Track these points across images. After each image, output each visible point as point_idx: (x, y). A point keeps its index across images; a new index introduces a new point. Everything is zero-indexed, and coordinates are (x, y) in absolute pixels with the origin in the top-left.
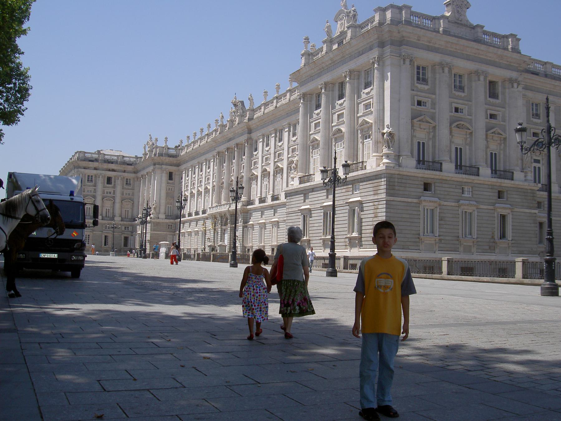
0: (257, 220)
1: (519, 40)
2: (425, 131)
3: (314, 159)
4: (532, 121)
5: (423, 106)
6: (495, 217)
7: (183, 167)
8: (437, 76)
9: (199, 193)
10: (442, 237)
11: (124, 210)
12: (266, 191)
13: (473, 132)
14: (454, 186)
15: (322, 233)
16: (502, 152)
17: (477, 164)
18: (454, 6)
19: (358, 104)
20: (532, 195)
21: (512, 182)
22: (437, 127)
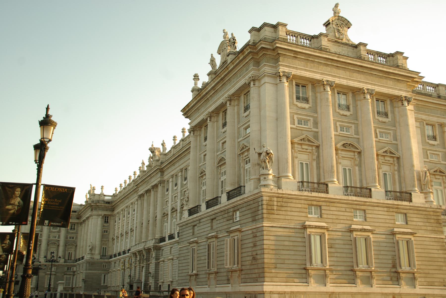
0: (167, 256)
1: (406, 58)
2: (308, 151)
3: (204, 190)
4: (428, 143)
5: (305, 125)
6: (394, 243)
7: (116, 212)
8: (318, 95)
9: (127, 233)
10: (333, 268)
11: (67, 253)
12: (175, 228)
13: (362, 152)
14: (344, 209)
15: (207, 267)
16: (396, 173)
17: (369, 186)
18: (334, 26)
19: (239, 128)
20: (435, 218)
21: (411, 204)
22: (321, 147)
